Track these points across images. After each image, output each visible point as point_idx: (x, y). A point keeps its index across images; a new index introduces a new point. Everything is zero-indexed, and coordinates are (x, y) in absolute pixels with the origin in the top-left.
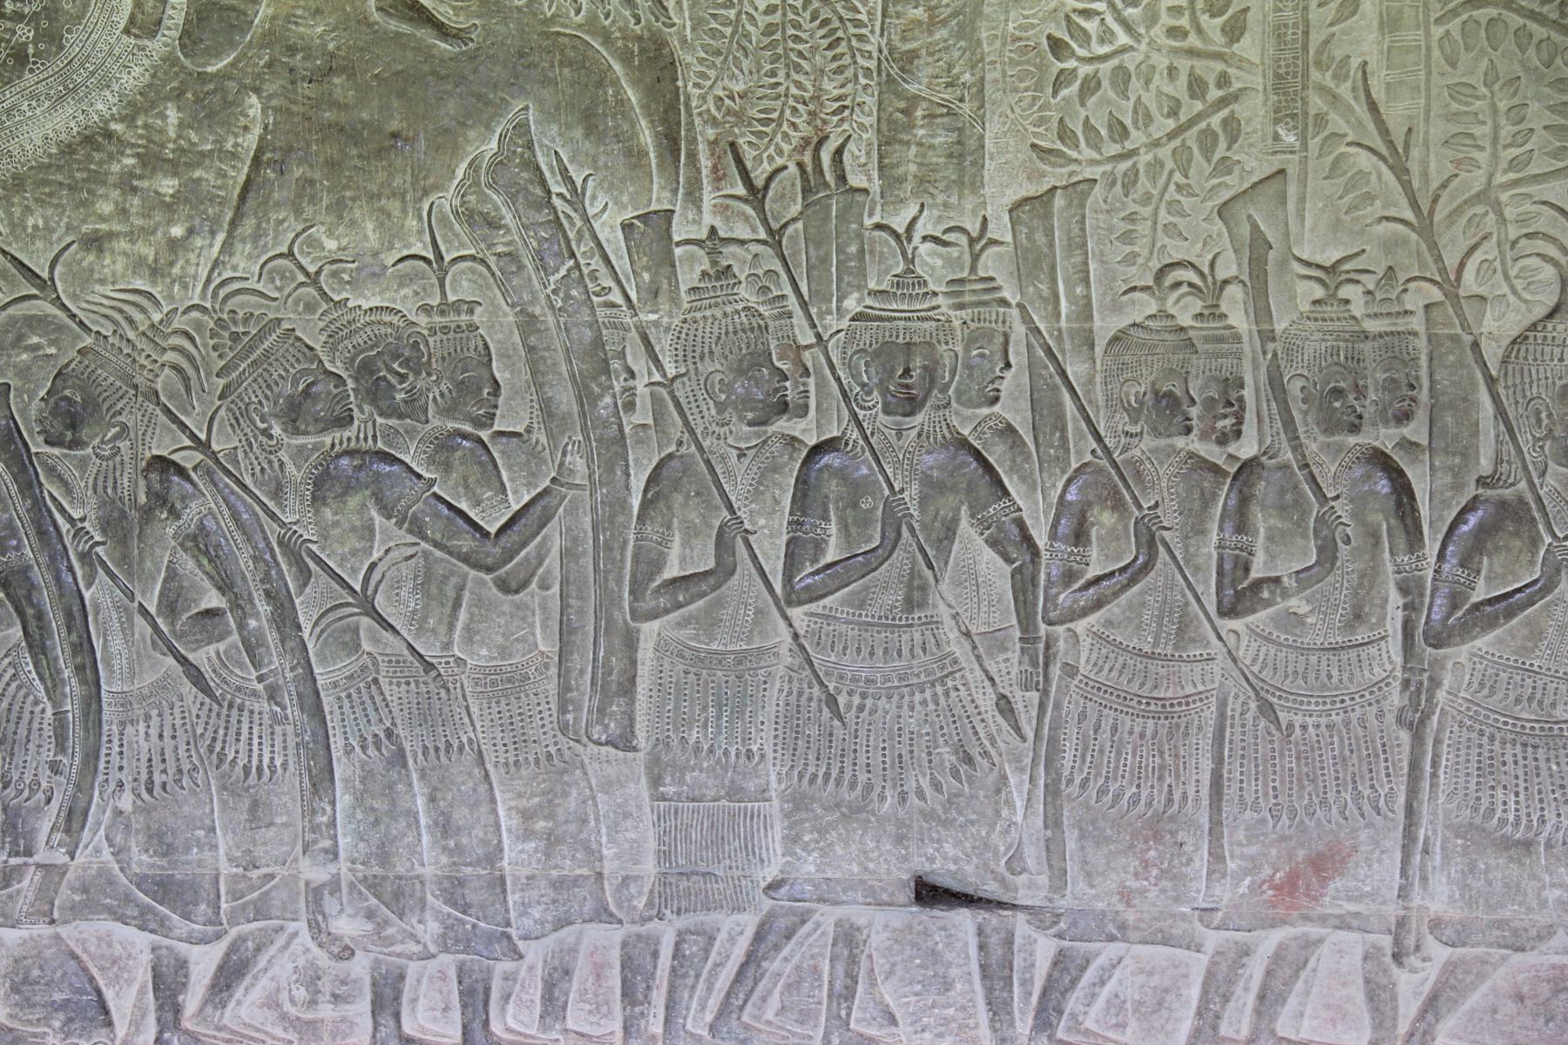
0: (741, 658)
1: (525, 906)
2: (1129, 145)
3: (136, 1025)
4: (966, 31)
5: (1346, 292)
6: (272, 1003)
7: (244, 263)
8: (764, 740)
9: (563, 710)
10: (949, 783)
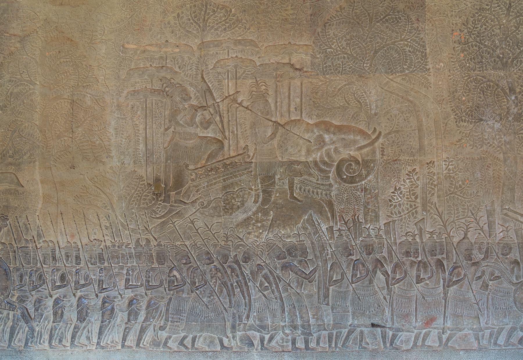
0: (345, 292)
1: (313, 329)
3: (258, 346)
4: (376, 199)
5: (434, 236)
6: (277, 342)
7: (271, 235)
8: (348, 304)
9: (318, 300)
10: (376, 309)
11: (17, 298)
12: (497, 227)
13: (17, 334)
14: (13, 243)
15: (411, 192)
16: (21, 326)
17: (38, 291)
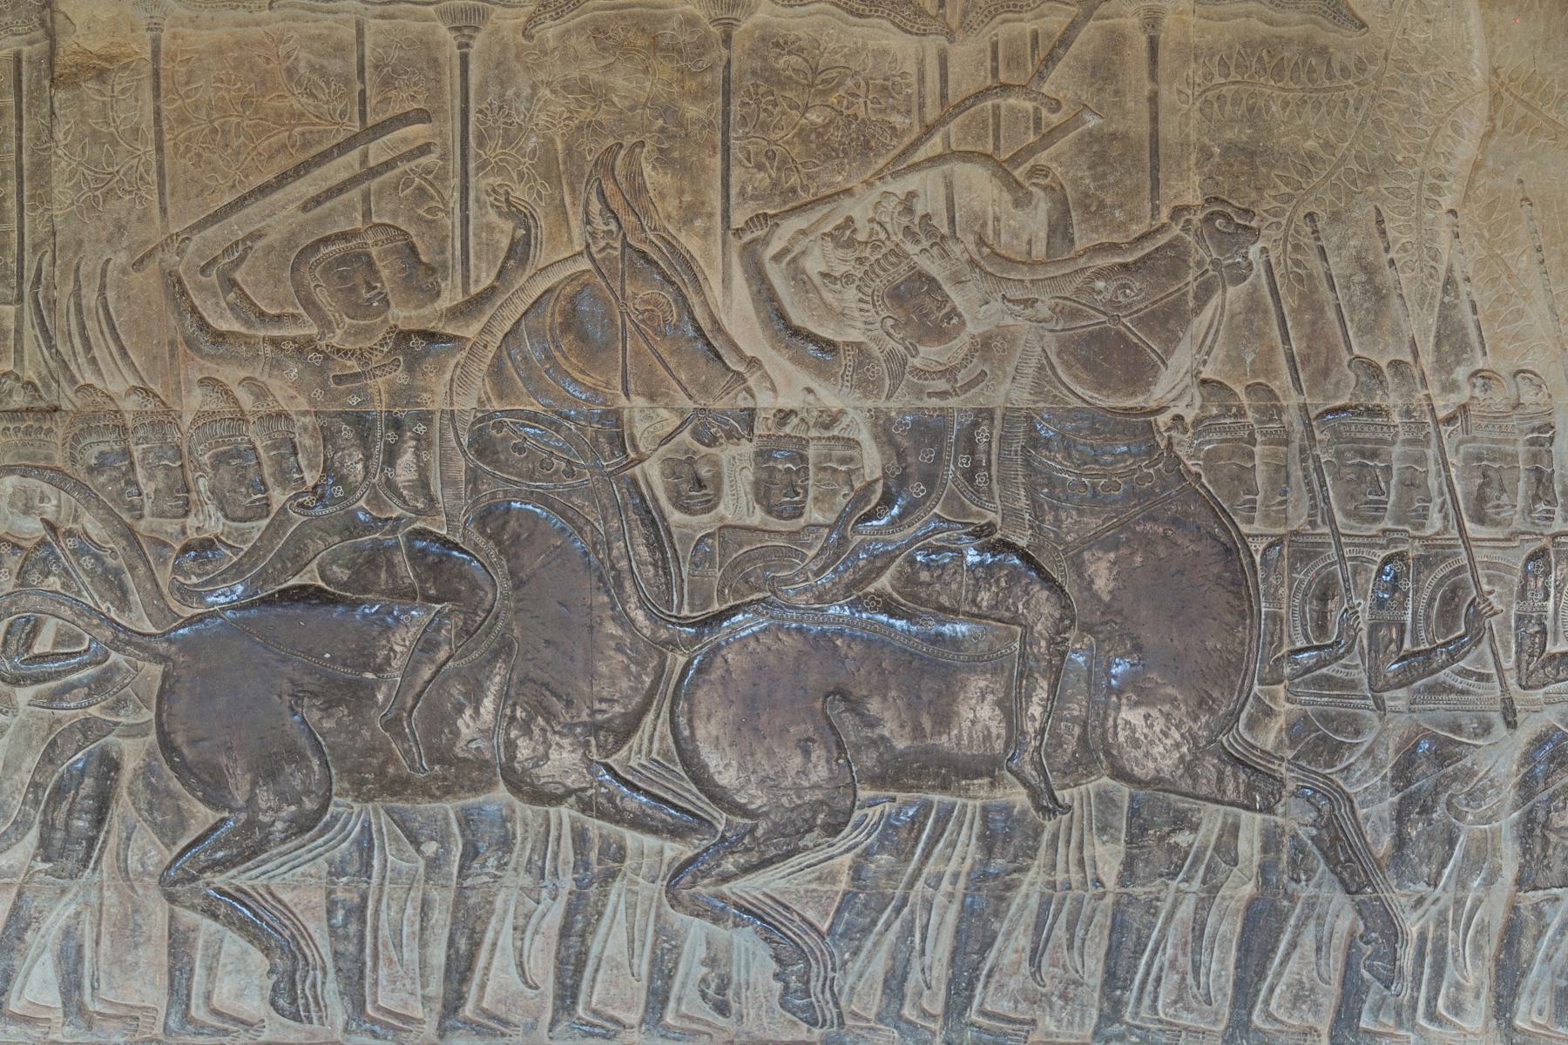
11: (1290, 727)
13: (1283, 963)
14: (1282, 381)
16: (1311, 904)
17: (1431, 689)
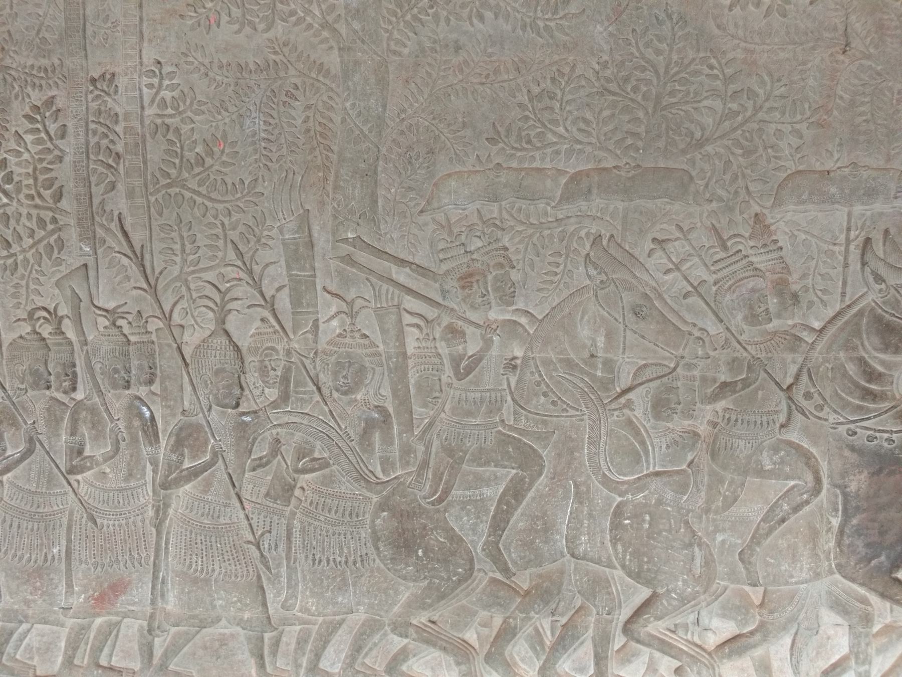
2: (12, 251)
5: (120, 322)
12: (320, 301)
15: (41, 178)
